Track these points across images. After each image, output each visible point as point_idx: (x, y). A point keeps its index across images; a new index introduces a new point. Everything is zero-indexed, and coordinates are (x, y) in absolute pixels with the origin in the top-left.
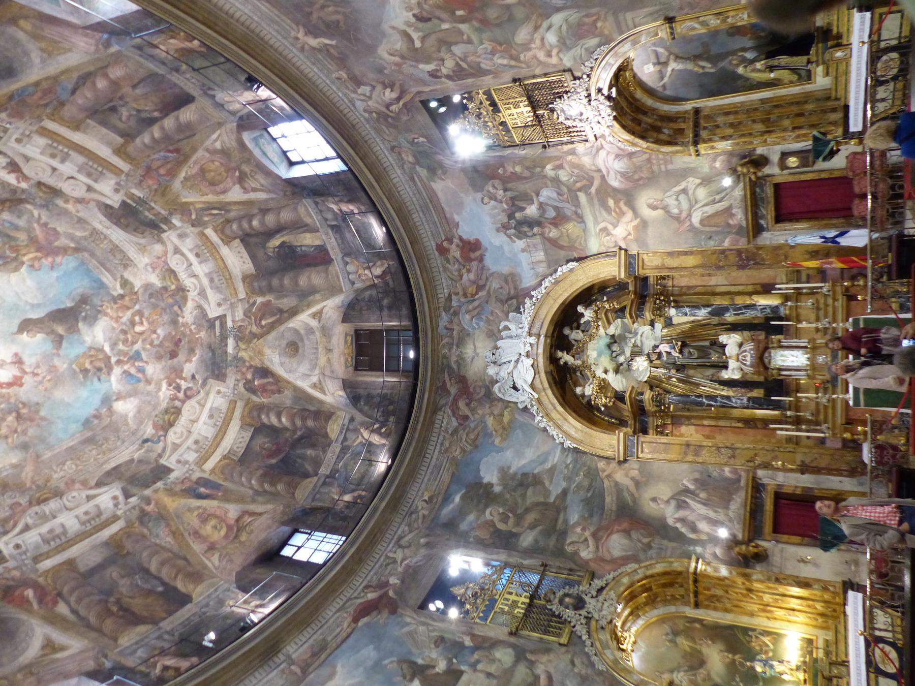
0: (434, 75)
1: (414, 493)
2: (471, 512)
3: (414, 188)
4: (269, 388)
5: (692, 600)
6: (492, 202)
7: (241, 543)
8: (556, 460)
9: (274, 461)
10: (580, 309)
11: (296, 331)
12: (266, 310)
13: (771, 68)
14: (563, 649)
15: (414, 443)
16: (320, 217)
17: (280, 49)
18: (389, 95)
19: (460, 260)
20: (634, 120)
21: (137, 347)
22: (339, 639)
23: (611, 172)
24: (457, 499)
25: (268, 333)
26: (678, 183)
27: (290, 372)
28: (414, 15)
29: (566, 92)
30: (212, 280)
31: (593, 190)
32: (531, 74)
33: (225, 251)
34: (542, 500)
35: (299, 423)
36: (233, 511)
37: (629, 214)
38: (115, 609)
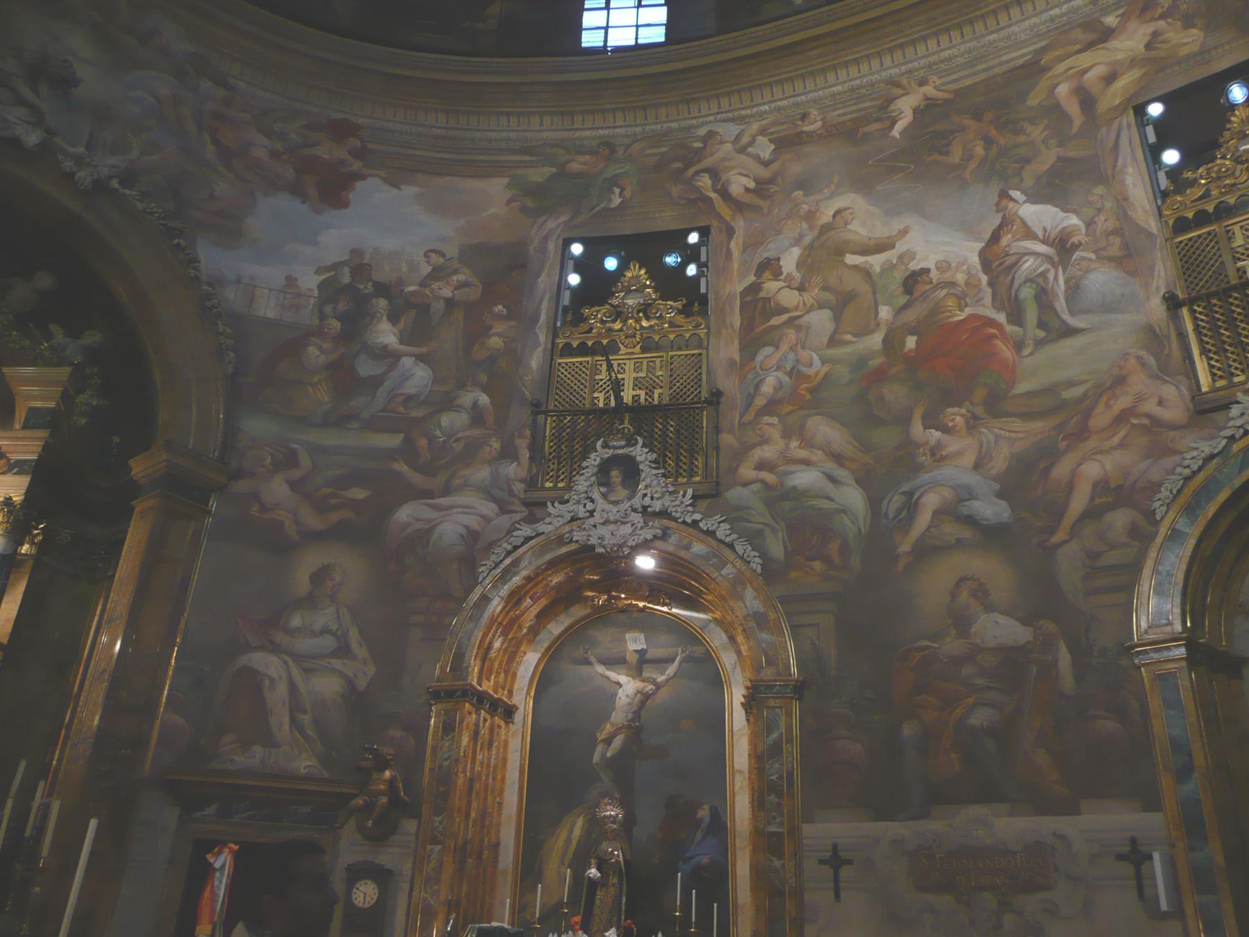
0: (770, 267)
6: (426, 269)
10: (92, 338)
17: (909, 51)
18: (739, 184)
31: (401, 467)
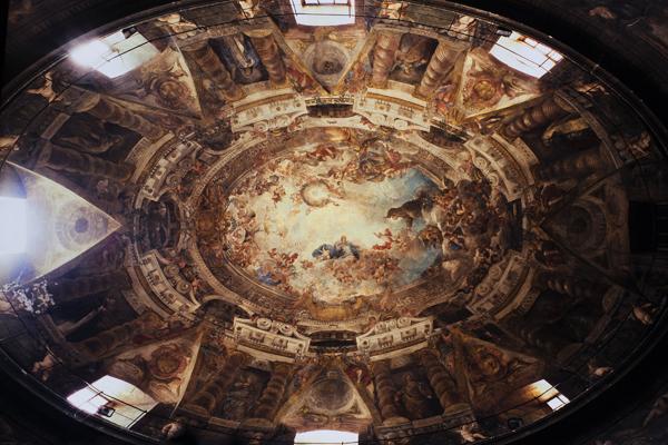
7: (507, 382)
9: (551, 322)
21: (459, 224)
30: (506, 173)
35: (578, 291)
38: (397, 399)
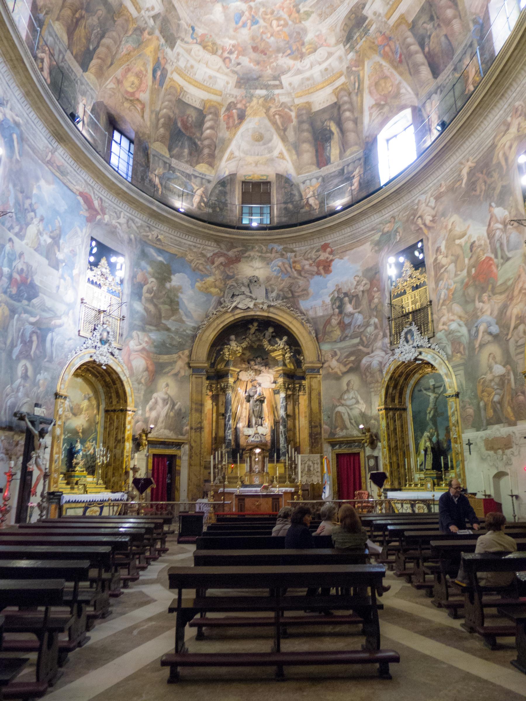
0: (438, 250)
1: (162, 228)
2: (152, 268)
3: (367, 230)
4: (231, 121)
5: (109, 409)
6: (355, 283)
7: (123, 103)
8: (188, 323)
9: (179, 125)
10: (285, 338)
11: (270, 140)
12: (286, 119)
13: (426, 451)
14: (77, 333)
15: (195, 227)
16: (350, 161)
17: (462, 148)
18: (428, 219)
19: (318, 259)
20: (402, 373)
21: (261, 22)
22: (69, 184)
23: (371, 359)
24: (160, 259)
25: (270, 120)
26: (362, 398)
27: (242, 136)
28: (474, 242)
29: (421, 333)
30: (308, 79)
31: (361, 347)
32: (434, 311)
33: (329, 90)
34: (163, 315)
35: (206, 142)
36: (144, 96)
37: (345, 369)
38: (77, 15)
